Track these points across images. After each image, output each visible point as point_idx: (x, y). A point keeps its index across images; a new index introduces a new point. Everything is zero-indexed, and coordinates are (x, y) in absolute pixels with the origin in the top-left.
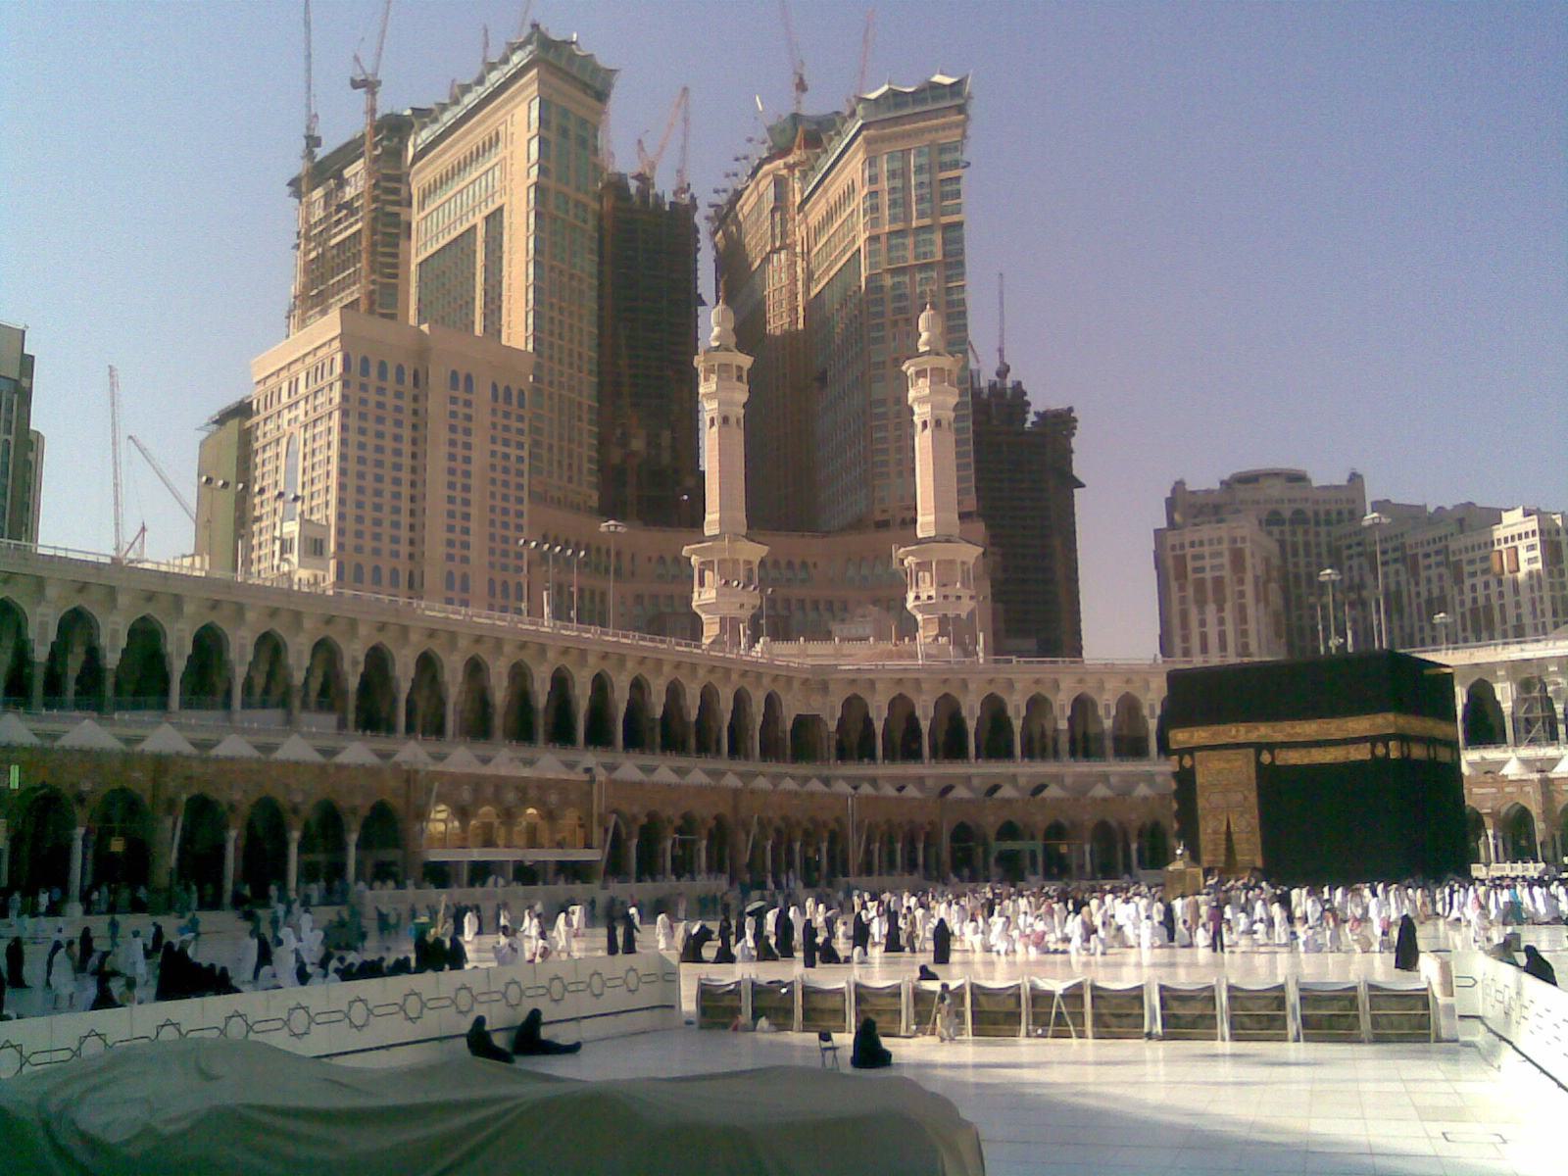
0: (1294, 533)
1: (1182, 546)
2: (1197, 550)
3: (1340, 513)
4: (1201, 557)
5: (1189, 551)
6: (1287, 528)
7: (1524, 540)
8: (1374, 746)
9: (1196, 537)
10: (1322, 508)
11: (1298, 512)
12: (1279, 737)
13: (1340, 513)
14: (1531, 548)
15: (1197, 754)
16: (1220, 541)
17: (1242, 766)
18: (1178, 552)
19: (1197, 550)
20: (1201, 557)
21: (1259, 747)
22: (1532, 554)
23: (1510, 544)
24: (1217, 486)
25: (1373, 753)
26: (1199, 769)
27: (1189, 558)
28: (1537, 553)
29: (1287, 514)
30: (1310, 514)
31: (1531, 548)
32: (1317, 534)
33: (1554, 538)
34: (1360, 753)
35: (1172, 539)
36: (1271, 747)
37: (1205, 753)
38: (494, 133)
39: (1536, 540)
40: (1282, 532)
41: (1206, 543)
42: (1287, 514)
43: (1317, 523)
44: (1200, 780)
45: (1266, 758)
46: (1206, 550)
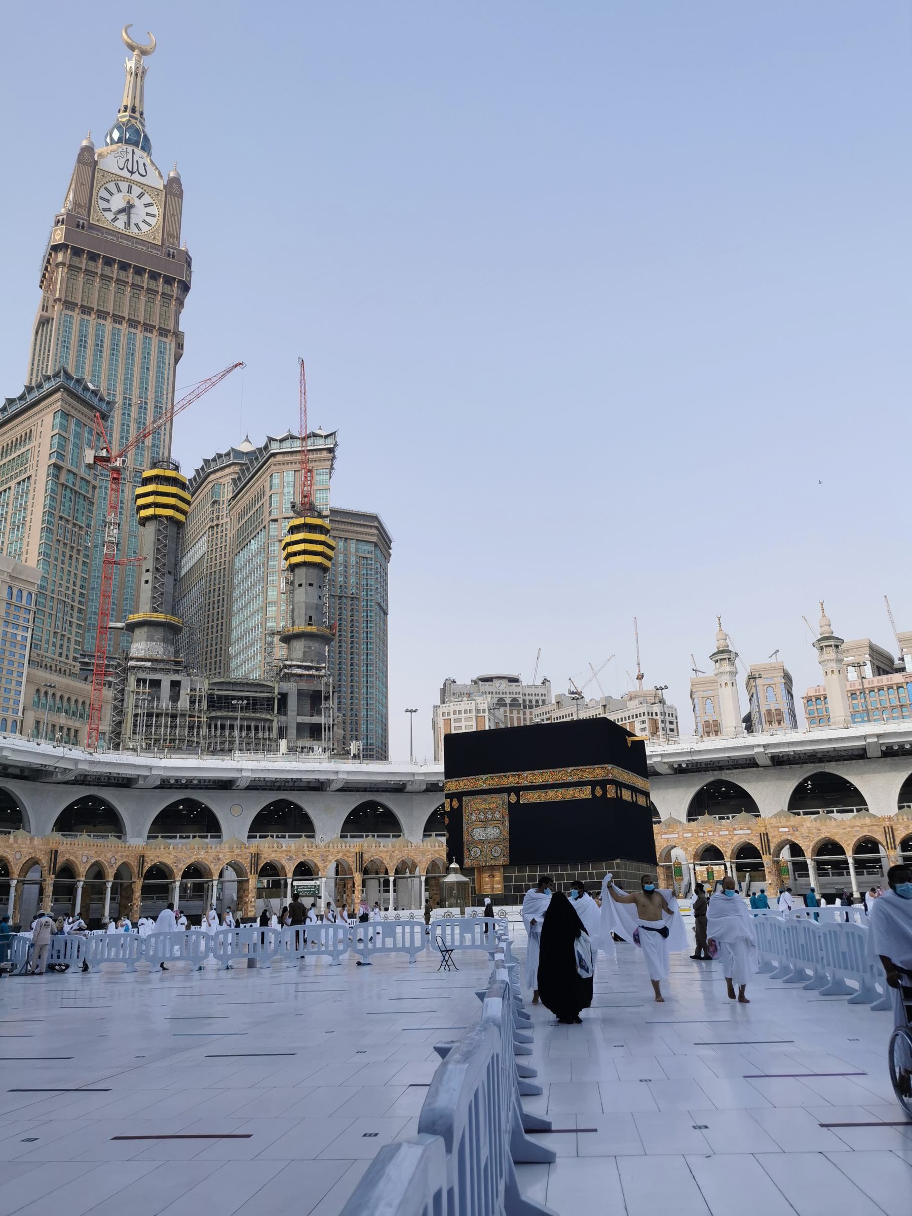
0: (511, 712)
1: (449, 713)
2: (457, 716)
3: (537, 701)
4: (459, 720)
5: (452, 717)
6: (508, 709)
7: (639, 718)
9: (457, 708)
10: (527, 698)
11: (514, 700)
13: (537, 701)
14: (644, 722)
15: (465, 799)
16: (470, 711)
17: (497, 806)
18: (447, 717)
19: (457, 716)
20: (459, 720)
21: (508, 790)
22: (643, 726)
23: (631, 720)
24: (469, 683)
25: (593, 793)
26: (466, 811)
27: (452, 721)
28: (646, 725)
29: (508, 701)
30: (521, 701)
31: (644, 722)
32: (524, 714)
33: (655, 717)
34: (585, 793)
35: (444, 709)
36: (517, 790)
37: (469, 798)
38: (28, 431)
39: (646, 718)
40: (505, 712)
41: (463, 712)
42: (508, 701)
43: (525, 707)
44: (465, 819)
45: (513, 798)
46: (463, 716)
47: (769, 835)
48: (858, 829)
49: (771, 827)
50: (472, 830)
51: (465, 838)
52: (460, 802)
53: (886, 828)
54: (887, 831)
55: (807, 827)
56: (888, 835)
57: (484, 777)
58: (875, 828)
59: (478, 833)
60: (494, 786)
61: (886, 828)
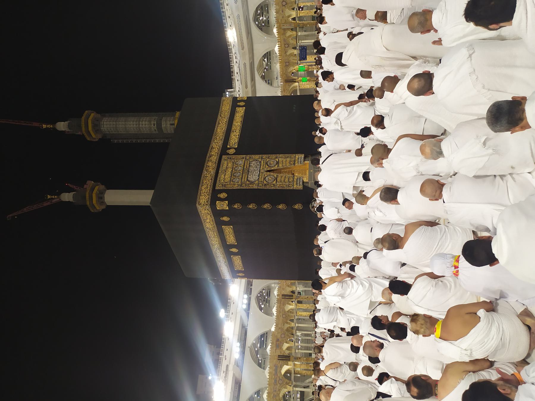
8: (240, 106)
12: (221, 143)
34: (240, 112)
47: (280, 355)
48: (281, 310)
49: (275, 353)
50: (249, 181)
51: (255, 187)
52: (221, 191)
53: (283, 297)
54: (284, 297)
55: (278, 334)
56: (286, 297)
57: (205, 172)
58: (282, 302)
59: (253, 177)
60: (215, 166)
61: (283, 297)
